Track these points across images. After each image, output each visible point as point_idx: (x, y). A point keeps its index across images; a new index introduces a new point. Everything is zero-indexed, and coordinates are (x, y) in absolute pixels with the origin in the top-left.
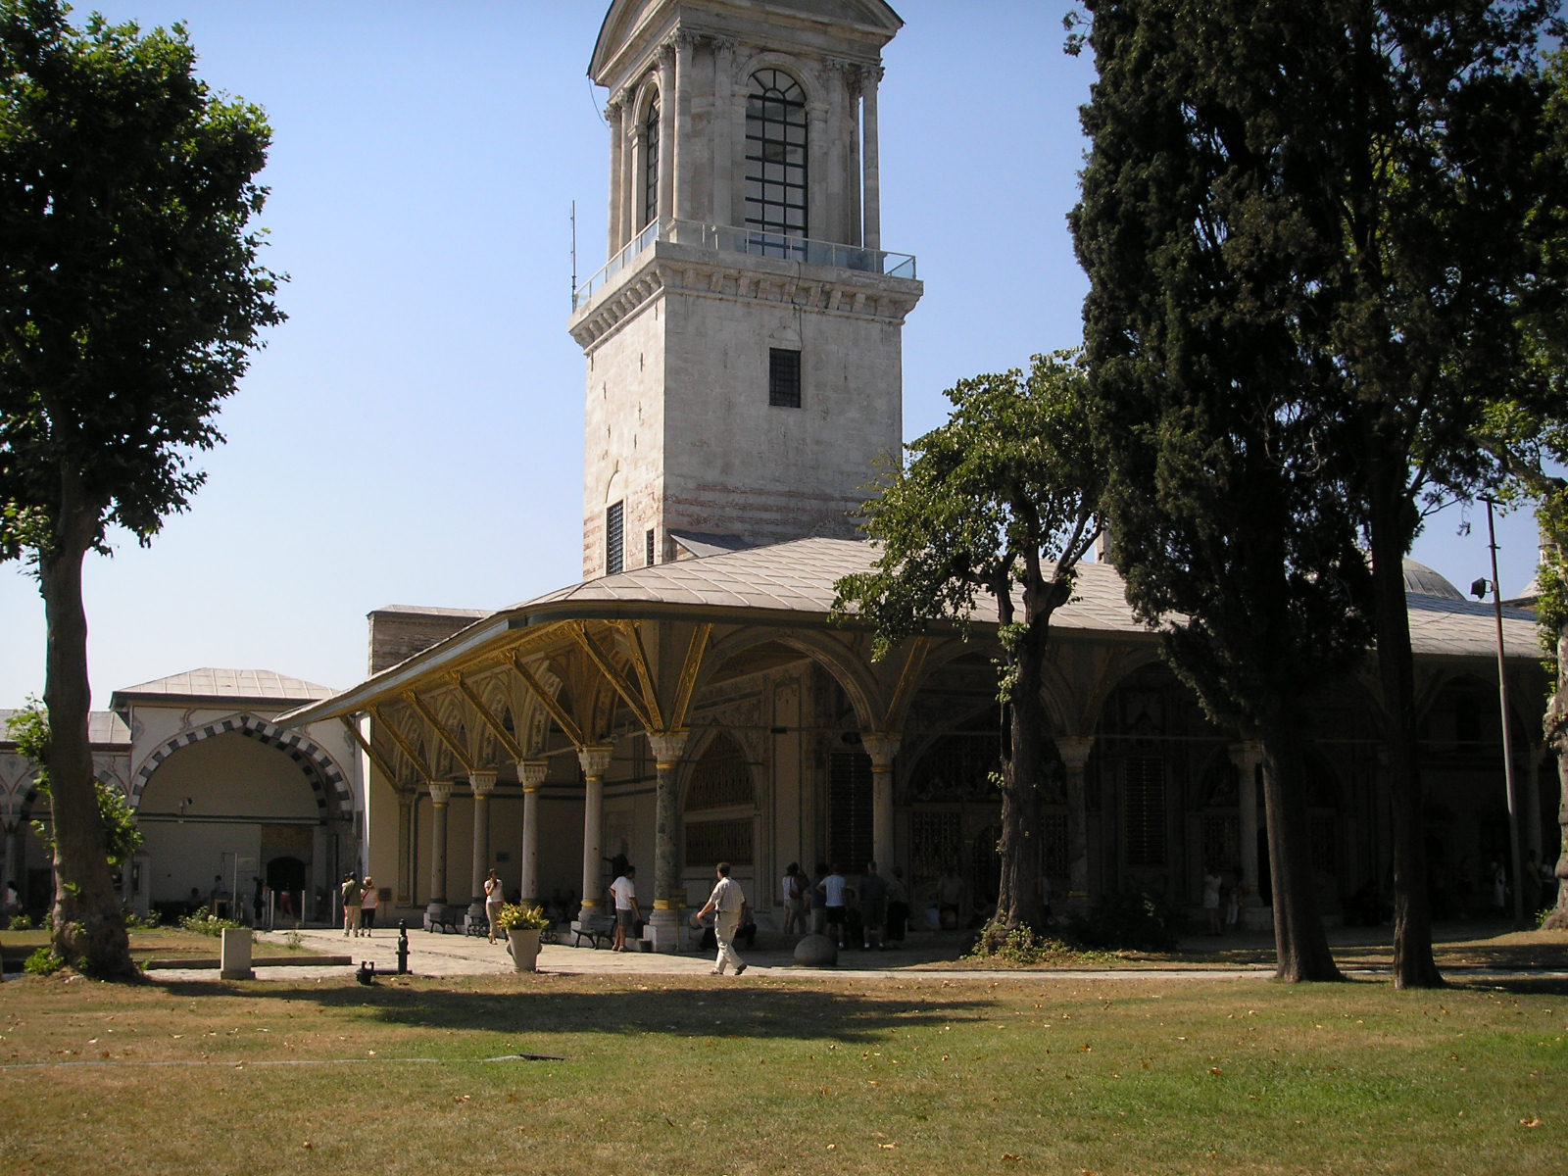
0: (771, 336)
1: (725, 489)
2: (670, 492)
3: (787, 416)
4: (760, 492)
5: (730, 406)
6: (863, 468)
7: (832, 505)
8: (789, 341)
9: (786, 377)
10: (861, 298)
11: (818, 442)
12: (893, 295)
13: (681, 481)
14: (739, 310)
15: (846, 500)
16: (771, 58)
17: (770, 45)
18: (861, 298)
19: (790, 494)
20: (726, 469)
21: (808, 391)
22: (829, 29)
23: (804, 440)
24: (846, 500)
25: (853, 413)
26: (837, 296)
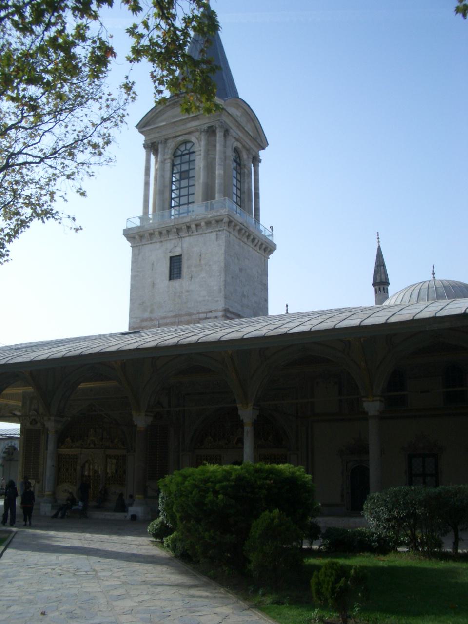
0: (170, 252)
1: (151, 320)
2: (131, 325)
3: (176, 283)
4: (164, 318)
5: (153, 284)
6: (207, 298)
7: (194, 317)
8: (177, 252)
9: (175, 267)
10: (203, 224)
11: (188, 291)
12: (216, 218)
13: (135, 320)
14: (158, 245)
15: (199, 313)
16: (180, 139)
17: (178, 134)
18: (203, 224)
19: (176, 316)
20: (151, 312)
21: (185, 270)
22: (199, 117)
23: (182, 292)
24: (199, 313)
25: (203, 275)
26: (193, 226)
